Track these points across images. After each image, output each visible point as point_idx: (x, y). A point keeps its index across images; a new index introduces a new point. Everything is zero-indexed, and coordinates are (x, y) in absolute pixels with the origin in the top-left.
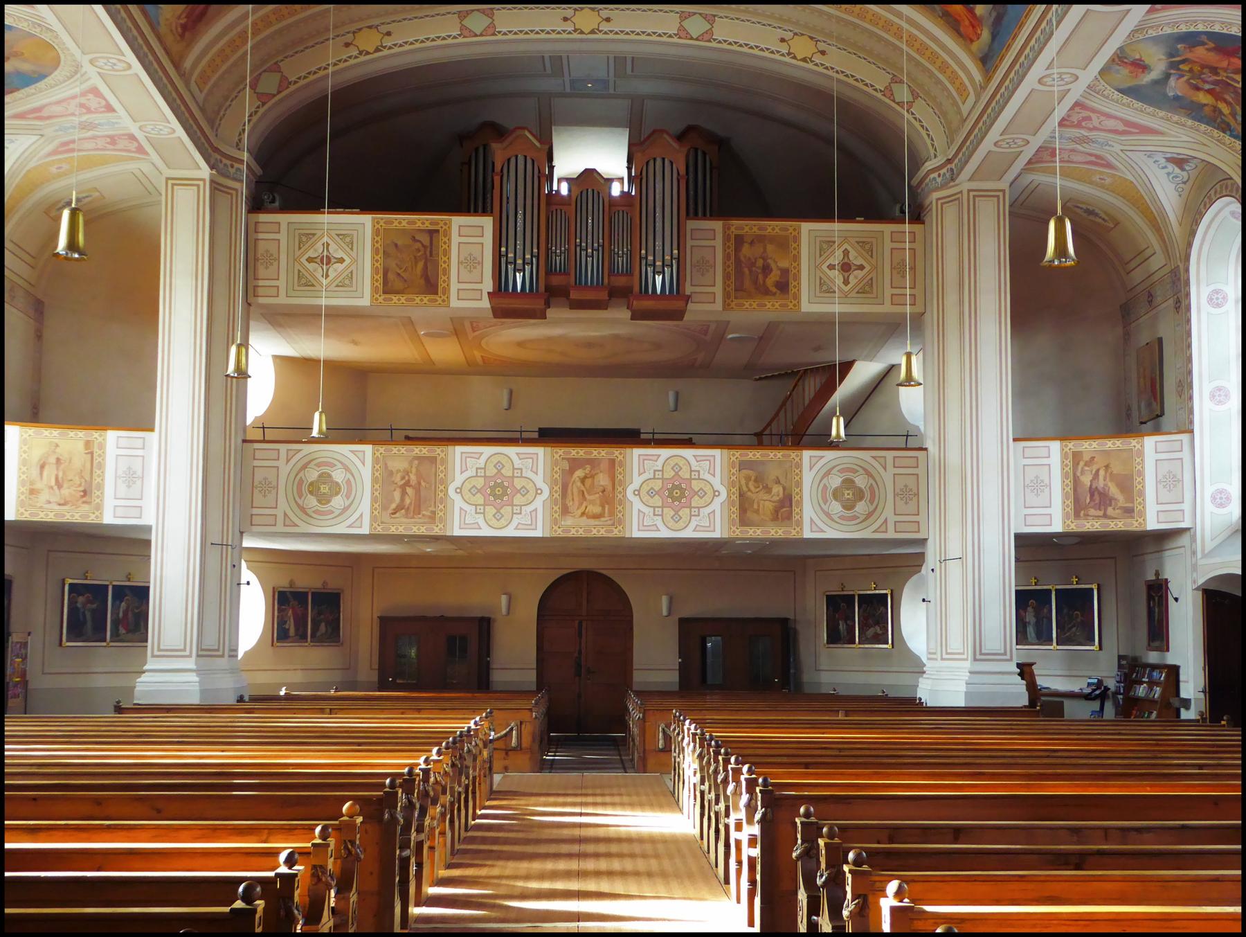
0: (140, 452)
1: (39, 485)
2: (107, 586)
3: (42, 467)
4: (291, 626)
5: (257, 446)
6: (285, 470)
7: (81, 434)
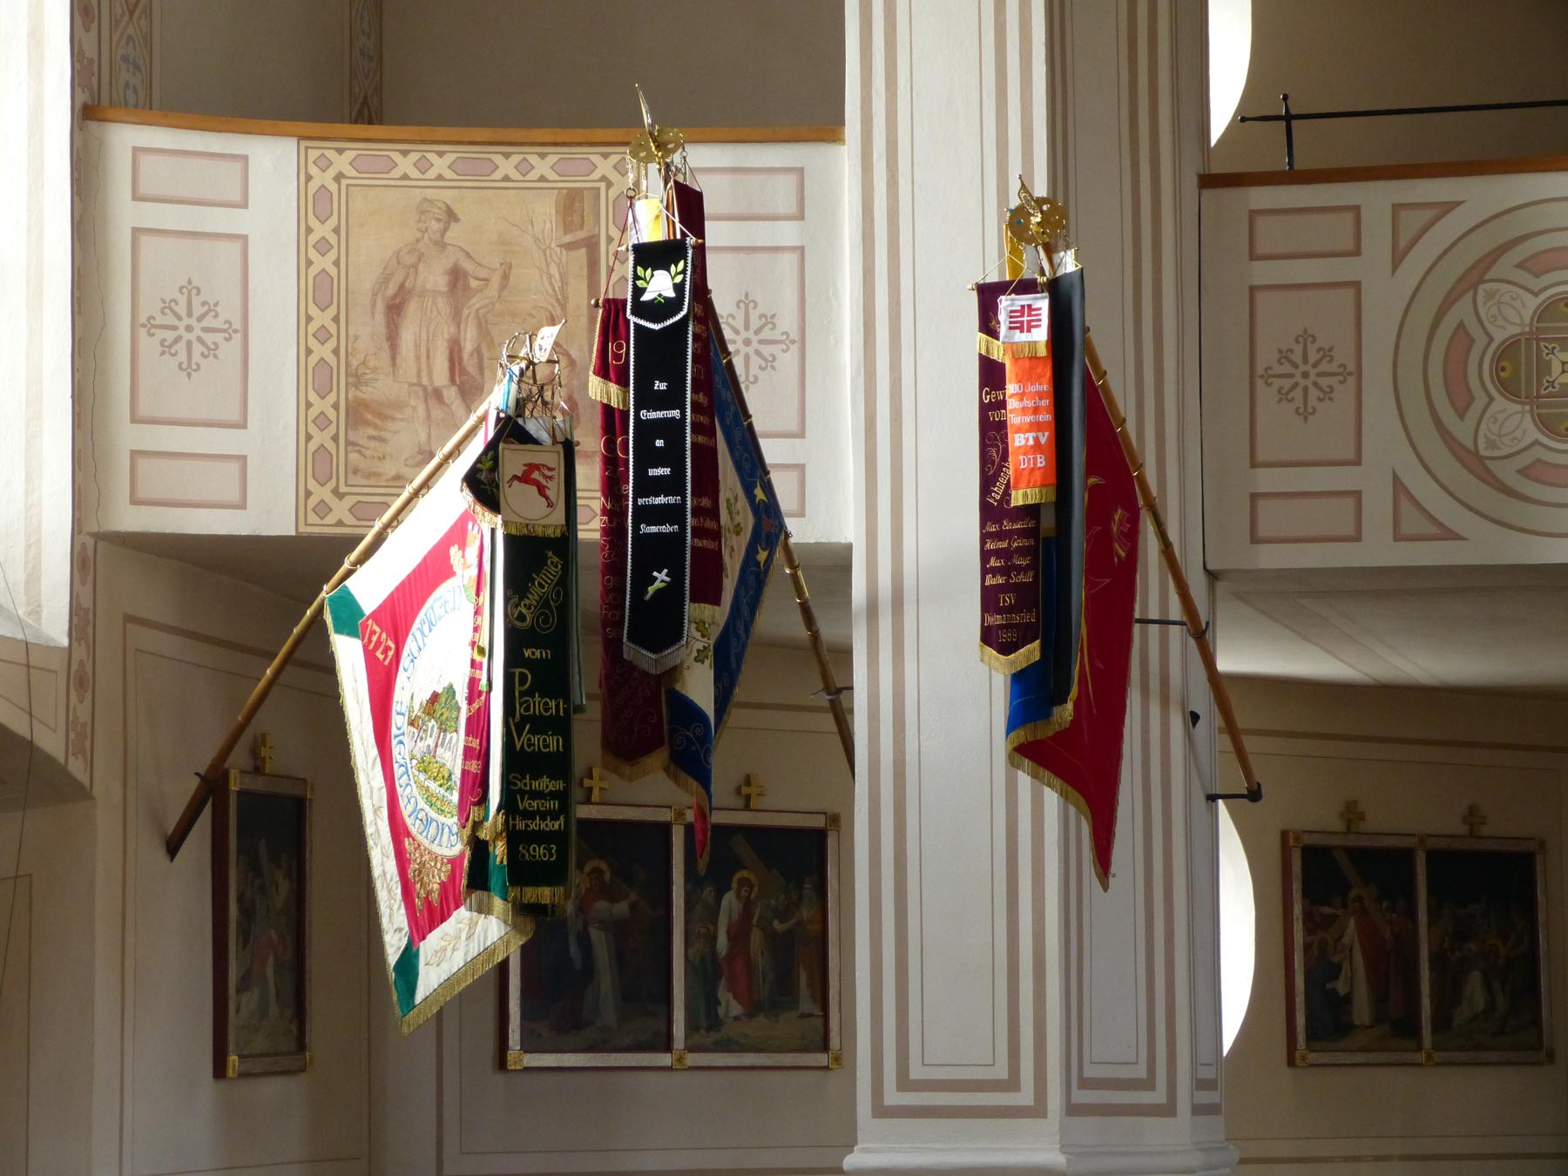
0: (787, 233)
1: (381, 388)
2: (665, 828)
3: (395, 310)
4: (1356, 982)
5: (1261, 197)
6: (1387, 294)
7: (544, 164)
